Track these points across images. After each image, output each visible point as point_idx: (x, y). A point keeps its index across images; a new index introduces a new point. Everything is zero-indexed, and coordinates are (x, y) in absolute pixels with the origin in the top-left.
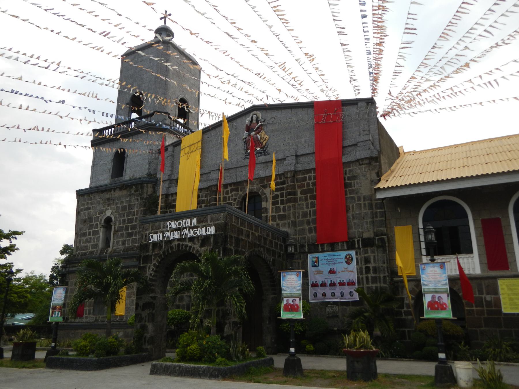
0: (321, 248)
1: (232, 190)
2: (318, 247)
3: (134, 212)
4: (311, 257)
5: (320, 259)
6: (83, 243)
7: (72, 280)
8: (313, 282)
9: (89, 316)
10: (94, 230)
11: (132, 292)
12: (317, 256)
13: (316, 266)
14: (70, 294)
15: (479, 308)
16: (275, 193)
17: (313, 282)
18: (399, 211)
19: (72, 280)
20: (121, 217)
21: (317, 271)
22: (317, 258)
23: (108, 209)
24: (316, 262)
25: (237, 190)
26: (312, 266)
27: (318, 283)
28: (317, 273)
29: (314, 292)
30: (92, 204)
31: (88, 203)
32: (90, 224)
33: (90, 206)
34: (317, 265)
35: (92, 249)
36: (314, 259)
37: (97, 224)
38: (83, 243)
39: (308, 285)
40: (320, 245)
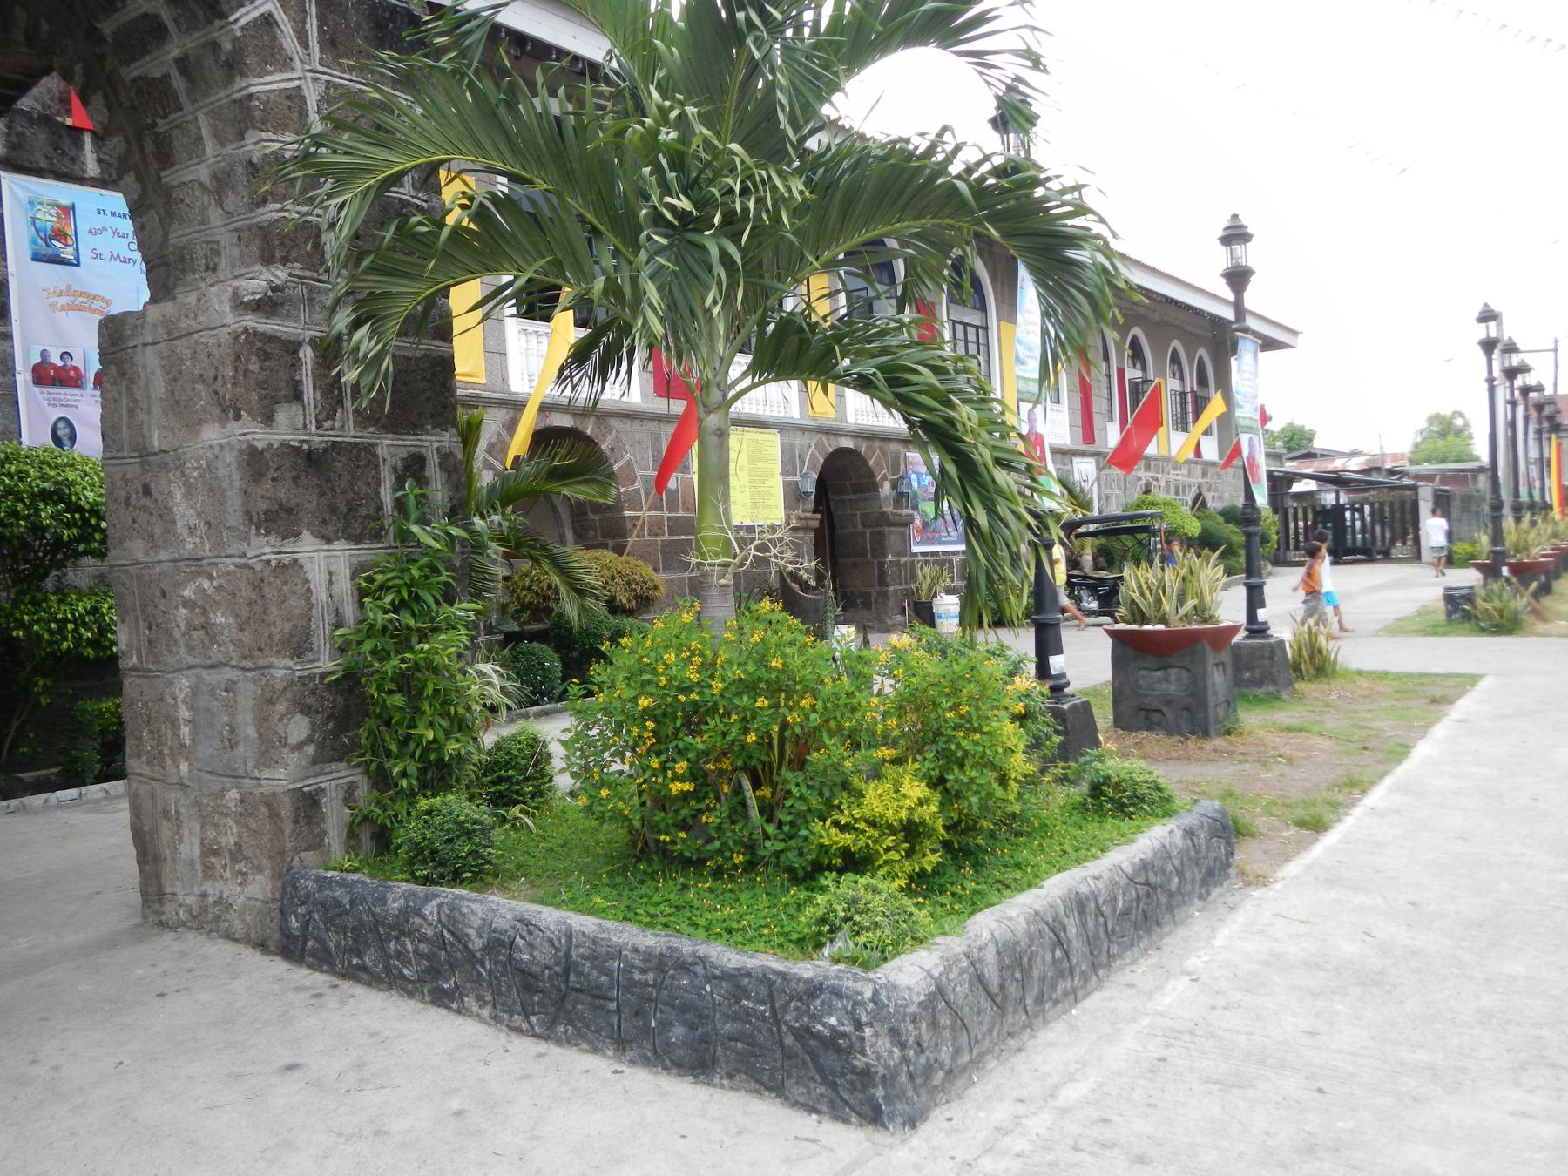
0: (100, 161)
2: (79, 145)
4: (23, 196)
5: (83, 227)
8: (44, 354)
12: (64, 202)
13: (64, 262)
15: (653, 513)
17: (44, 354)
18: (470, 99)
21: (68, 292)
22: (67, 211)
24: (59, 235)
26: (37, 258)
27: (77, 362)
28: (71, 307)
29: (57, 413)
34: (68, 254)
36: (48, 218)
39: (10, 371)
40: (87, 138)
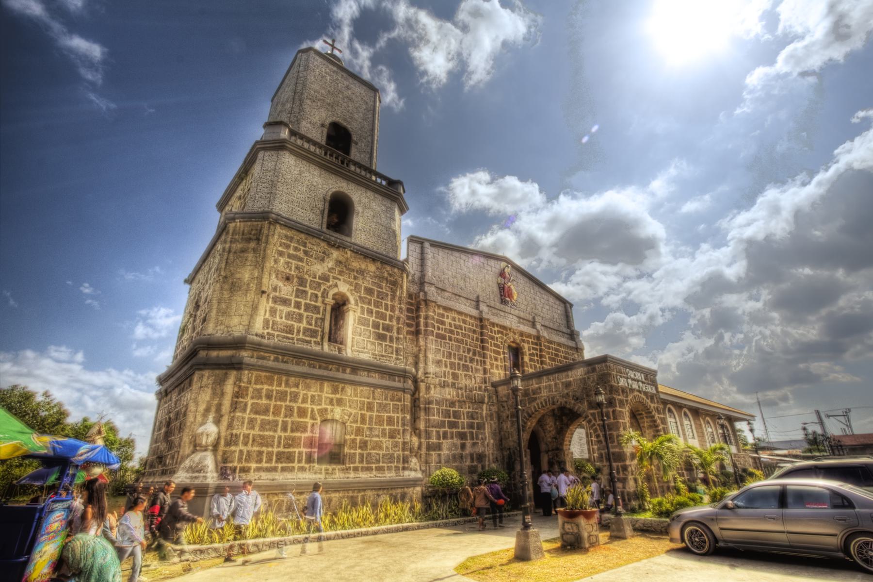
1: (499, 332)
3: (386, 305)
6: (281, 318)
7: (258, 387)
9: (307, 466)
10: (308, 301)
11: (395, 429)
14: (253, 416)
16: (532, 351)
19: (258, 387)
20: (364, 303)
23: (340, 280)
25: (502, 333)
30: (306, 253)
31: (296, 249)
32: (301, 288)
33: (301, 254)
35: (304, 333)
37: (316, 296)
38: (281, 318)
